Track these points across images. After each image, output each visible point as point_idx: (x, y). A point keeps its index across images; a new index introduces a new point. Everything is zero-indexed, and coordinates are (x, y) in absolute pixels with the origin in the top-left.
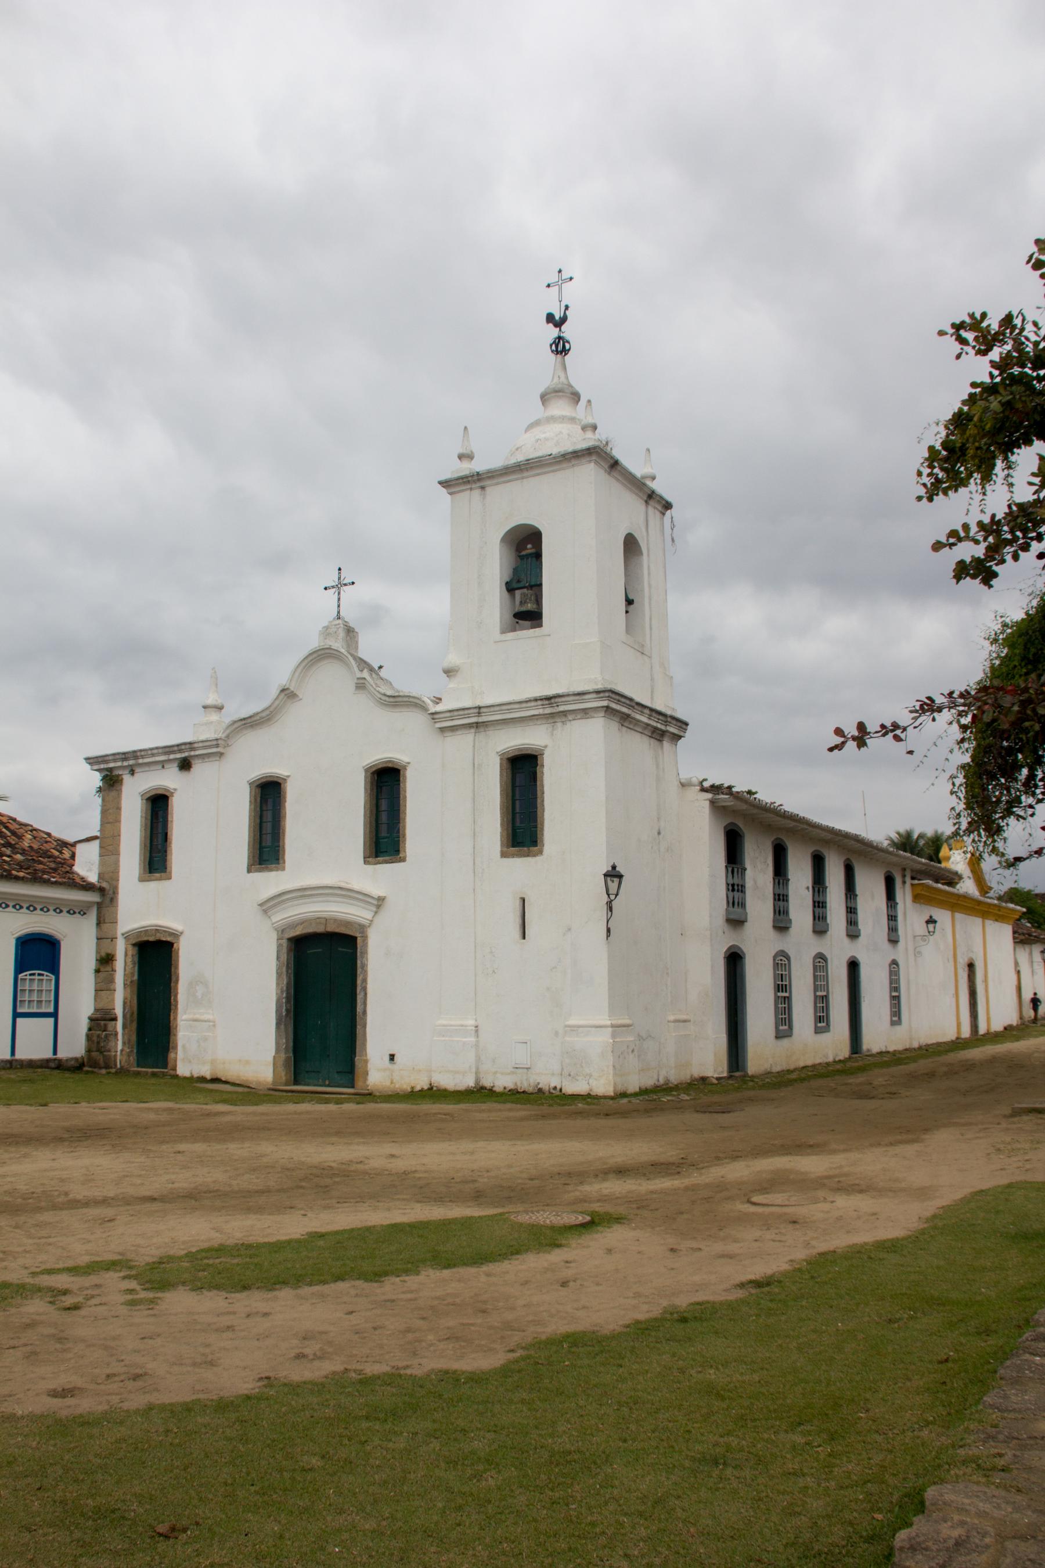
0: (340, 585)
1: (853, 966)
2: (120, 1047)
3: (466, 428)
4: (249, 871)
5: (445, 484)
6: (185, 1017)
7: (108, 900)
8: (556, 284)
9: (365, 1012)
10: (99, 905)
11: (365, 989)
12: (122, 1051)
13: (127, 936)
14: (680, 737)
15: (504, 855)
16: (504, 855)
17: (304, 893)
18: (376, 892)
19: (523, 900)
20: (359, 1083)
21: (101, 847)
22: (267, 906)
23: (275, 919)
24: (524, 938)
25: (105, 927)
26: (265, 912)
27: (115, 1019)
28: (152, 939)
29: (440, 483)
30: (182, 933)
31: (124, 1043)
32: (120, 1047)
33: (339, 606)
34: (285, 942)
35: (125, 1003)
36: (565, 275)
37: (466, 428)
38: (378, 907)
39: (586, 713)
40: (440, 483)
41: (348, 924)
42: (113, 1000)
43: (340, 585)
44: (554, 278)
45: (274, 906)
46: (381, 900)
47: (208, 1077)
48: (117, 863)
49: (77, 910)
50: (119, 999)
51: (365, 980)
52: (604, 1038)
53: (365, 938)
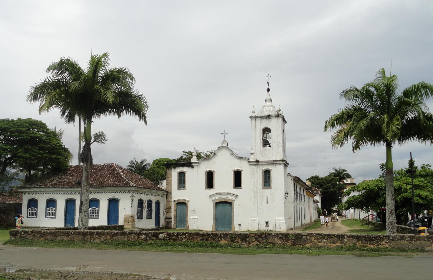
0: (225, 134)
1: (301, 208)
2: (173, 224)
3: (254, 106)
4: (206, 189)
5: (251, 117)
6: (191, 218)
7: (169, 194)
8: (267, 77)
9: (234, 217)
10: (167, 195)
11: (234, 212)
12: (174, 225)
13: (174, 201)
14: (287, 166)
15: (263, 188)
16: (263, 188)
17: (220, 194)
18: (237, 194)
19: (267, 197)
20: (233, 230)
21: (166, 182)
22: (210, 196)
23: (212, 199)
24: (267, 203)
25: (168, 199)
26: (210, 197)
27: (172, 218)
28: (181, 202)
29: (250, 117)
30: (189, 201)
31: (174, 223)
32: (173, 224)
33: (225, 138)
34: (215, 203)
35: (174, 215)
36: (270, 76)
37: (254, 106)
38: (236, 197)
39: (280, 164)
40: (250, 117)
41: (230, 200)
42: (171, 215)
43: (225, 134)
44: (267, 76)
45: (213, 196)
46: (237, 195)
47: (197, 230)
48: (171, 186)
49: (162, 196)
50: (172, 214)
51: (234, 211)
52: (284, 221)
53: (234, 203)
